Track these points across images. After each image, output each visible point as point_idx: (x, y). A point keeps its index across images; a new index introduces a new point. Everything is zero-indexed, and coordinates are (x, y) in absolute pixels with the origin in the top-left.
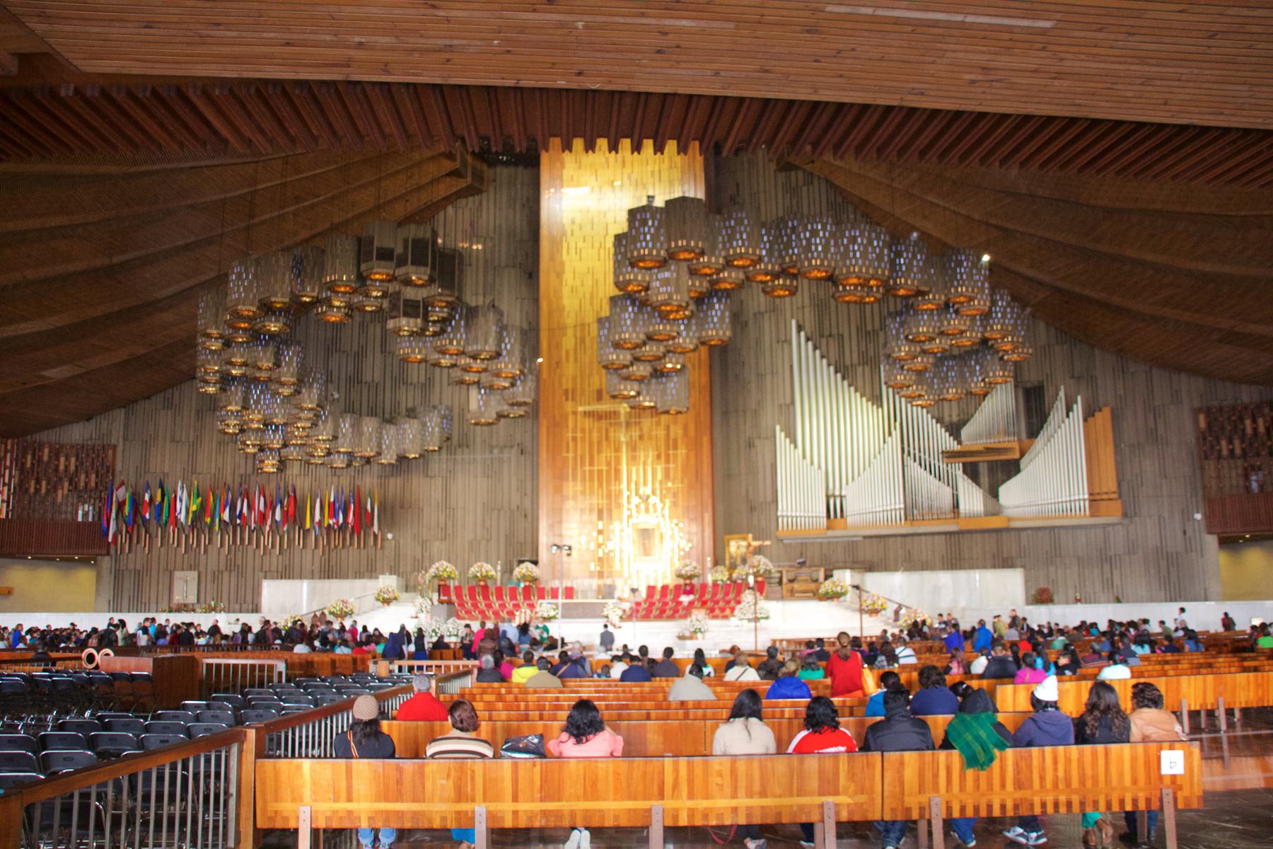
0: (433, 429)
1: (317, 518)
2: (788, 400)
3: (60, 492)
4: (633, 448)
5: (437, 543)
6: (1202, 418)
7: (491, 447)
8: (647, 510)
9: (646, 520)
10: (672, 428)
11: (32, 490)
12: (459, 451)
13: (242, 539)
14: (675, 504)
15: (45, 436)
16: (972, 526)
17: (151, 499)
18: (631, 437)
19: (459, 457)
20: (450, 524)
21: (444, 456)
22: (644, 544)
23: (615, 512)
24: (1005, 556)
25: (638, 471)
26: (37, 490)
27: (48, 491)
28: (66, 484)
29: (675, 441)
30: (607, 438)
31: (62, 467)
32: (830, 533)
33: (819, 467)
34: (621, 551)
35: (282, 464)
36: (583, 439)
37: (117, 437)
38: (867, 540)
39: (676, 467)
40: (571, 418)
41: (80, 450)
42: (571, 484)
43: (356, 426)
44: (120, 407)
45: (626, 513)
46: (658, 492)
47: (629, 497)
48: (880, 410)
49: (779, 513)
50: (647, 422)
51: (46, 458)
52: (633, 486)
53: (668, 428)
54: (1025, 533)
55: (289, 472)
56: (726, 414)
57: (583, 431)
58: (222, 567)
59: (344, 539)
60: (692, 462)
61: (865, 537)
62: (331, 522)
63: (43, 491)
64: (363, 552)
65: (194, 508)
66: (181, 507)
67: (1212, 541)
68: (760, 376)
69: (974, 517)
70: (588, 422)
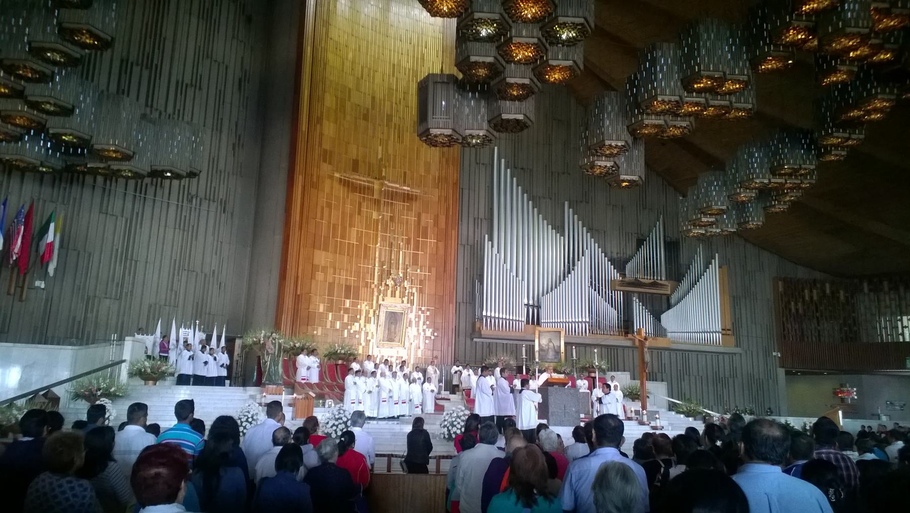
6: (780, 283)
10: (423, 216)
22: (389, 329)
23: (363, 292)
29: (426, 228)
30: (359, 214)
34: (367, 334)
39: (424, 257)
40: (328, 182)
48: (562, 237)
49: (484, 313)
50: (399, 205)
53: (419, 216)
60: (441, 252)
67: (781, 372)
70: (340, 191)
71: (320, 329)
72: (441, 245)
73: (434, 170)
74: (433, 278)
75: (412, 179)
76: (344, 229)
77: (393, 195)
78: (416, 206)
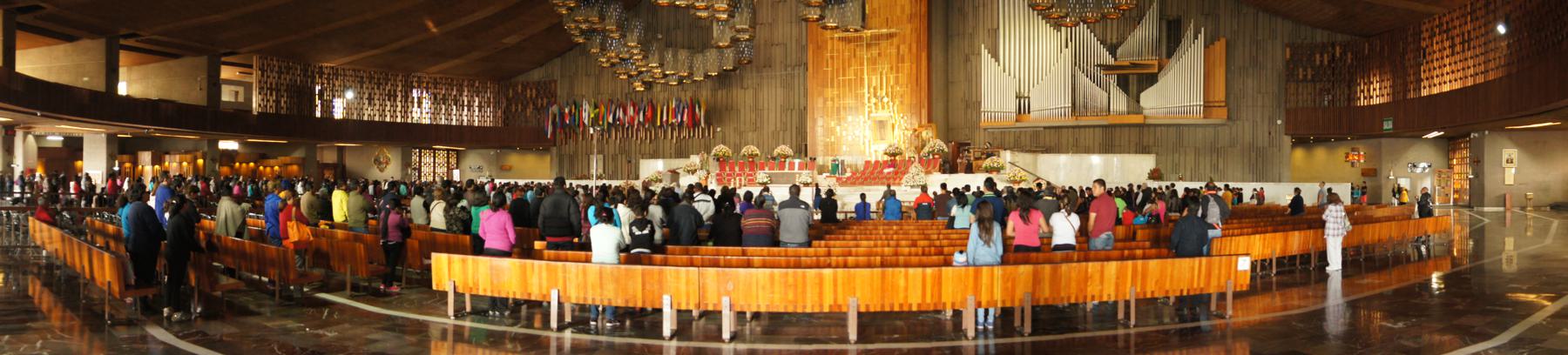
0: (729, 55)
1: (665, 118)
2: (995, 27)
3: (528, 110)
4: (873, 61)
5: (750, 134)
7: (786, 66)
8: (883, 108)
9: (882, 114)
10: (902, 47)
11: (513, 110)
12: (764, 70)
13: (628, 135)
14: (902, 102)
15: (521, 78)
16: (1118, 121)
17: (570, 111)
18: (872, 54)
19: (764, 74)
20: (759, 120)
21: (754, 74)
24: (1145, 144)
25: (877, 79)
26: (516, 110)
27: (522, 110)
28: (531, 106)
29: (903, 56)
31: (528, 96)
32: (1018, 125)
33: (1015, 77)
34: (864, 137)
35: (649, 86)
36: (838, 57)
37: (557, 74)
38: (1047, 131)
39: (903, 78)
40: (829, 42)
41: (538, 85)
42: (830, 90)
43: (675, 56)
44: (557, 57)
45: (867, 110)
46: (890, 94)
47: (869, 98)
49: (982, 109)
50: (884, 44)
51: (520, 91)
52: (872, 90)
54: (1159, 128)
55: (655, 90)
56: (948, 37)
57: (838, 51)
58: (617, 152)
59: (689, 133)
60: (914, 71)
61: (1045, 128)
62: (674, 121)
63: (520, 110)
64: (703, 141)
65: (592, 115)
66: (585, 115)
68: (976, 9)
69: (1120, 114)
71: (833, 137)
72: (914, 66)
73: (908, 11)
74: (909, 91)
75: (892, 21)
76: (844, 70)
77: (878, 38)
78: (895, 40)
